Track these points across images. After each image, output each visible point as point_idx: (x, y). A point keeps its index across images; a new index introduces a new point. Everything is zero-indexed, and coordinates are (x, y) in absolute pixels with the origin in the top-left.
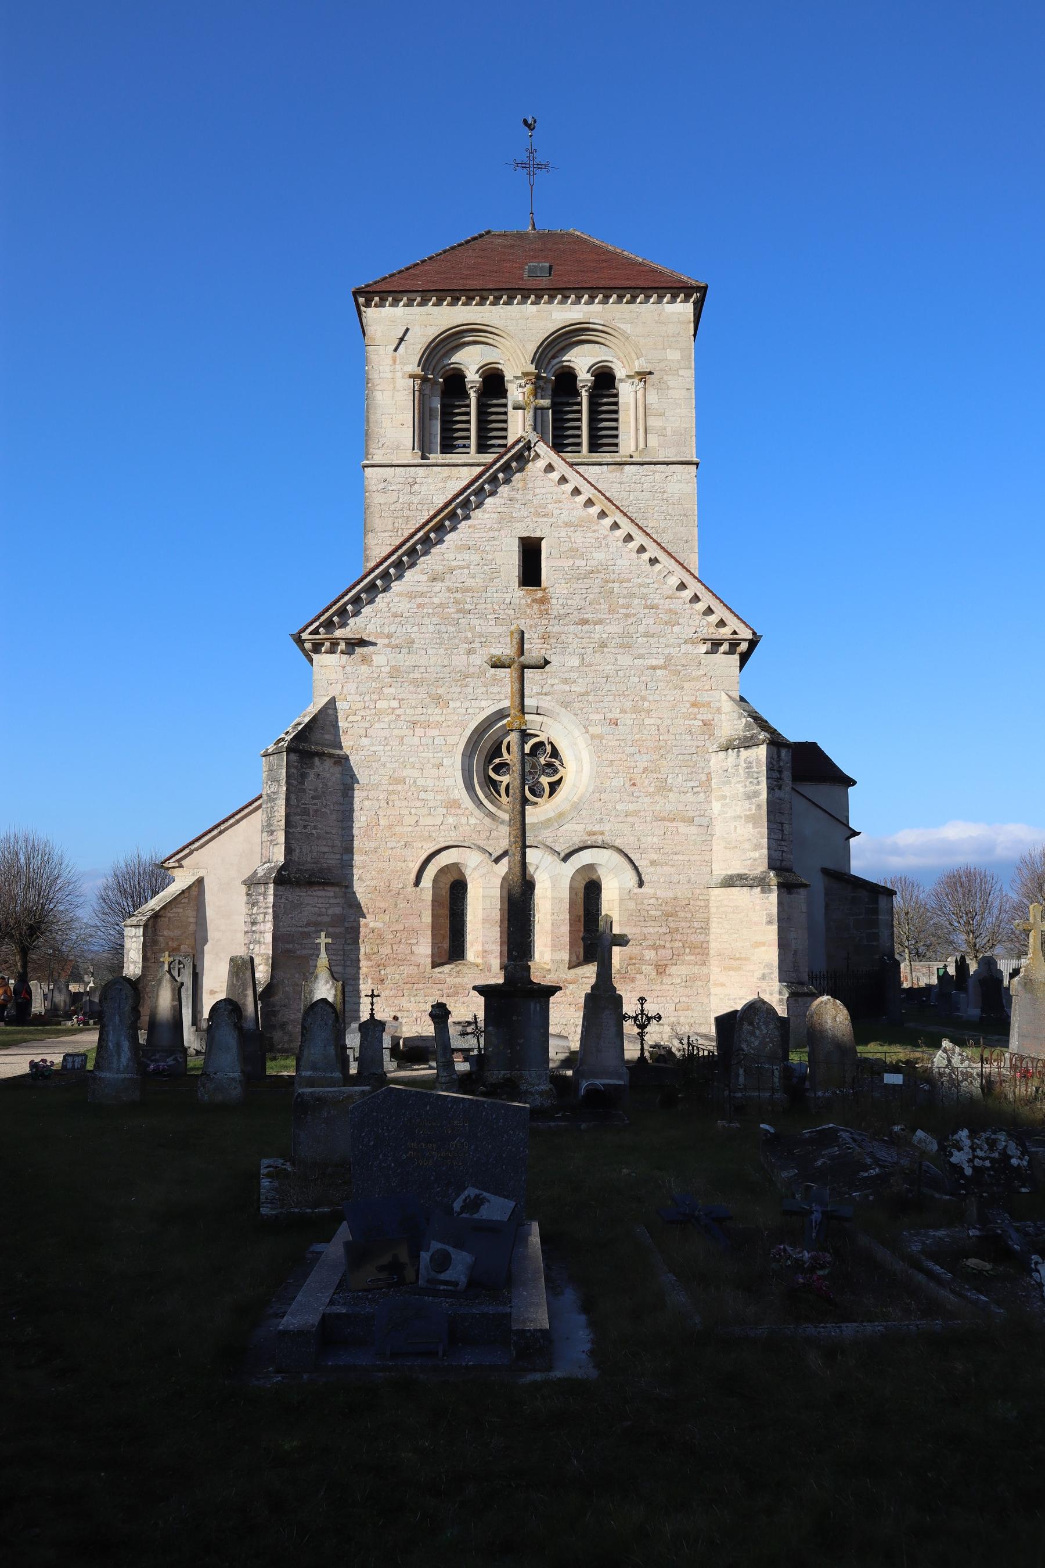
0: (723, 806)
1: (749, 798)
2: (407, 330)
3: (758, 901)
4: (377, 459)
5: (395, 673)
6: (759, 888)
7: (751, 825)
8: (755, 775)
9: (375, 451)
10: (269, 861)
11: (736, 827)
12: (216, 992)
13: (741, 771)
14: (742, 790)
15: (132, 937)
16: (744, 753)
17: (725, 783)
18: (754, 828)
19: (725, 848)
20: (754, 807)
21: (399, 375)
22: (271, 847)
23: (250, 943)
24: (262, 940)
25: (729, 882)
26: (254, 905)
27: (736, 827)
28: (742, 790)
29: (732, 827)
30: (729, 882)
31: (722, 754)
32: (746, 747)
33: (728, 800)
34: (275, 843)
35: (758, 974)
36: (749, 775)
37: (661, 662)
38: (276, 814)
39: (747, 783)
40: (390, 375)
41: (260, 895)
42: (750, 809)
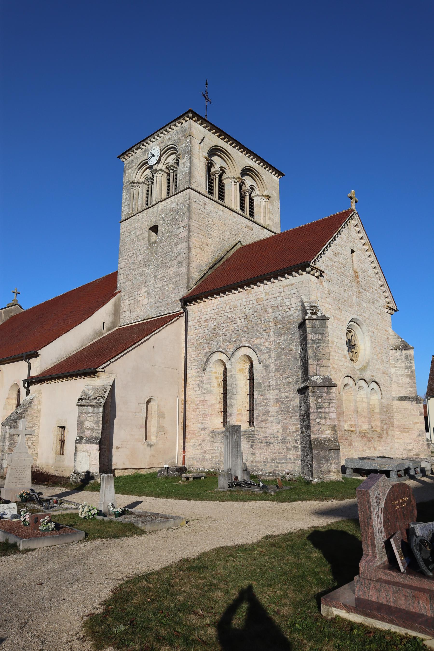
0: (396, 370)
1: (407, 368)
2: (204, 138)
3: (415, 407)
4: (194, 187)
5: (330, 293)
6: (415, 402)
7: (409, 378)
8: (410, 360)
9: (193, 183)
10: (316, 375)
11: (402, 379)
12: (119, 448)
13: (403, 358)
14: (404, 365)
15: (89, 413)
16: (404, 352)
17: (396, 362)
18: (410, 379)
19: (398, 386)
20: (410, 372)
21: (201, 155)
22: (318, 368)
23: (317, 418)
24: (327, 417)
25: (403, 399)
26: (318, 398)
27: (402, 379)
28: (404, 365)
29: (400, 379)
30: (403, 399)
31: (394, 351)
32: (405, 350)
33: (398, 368)
34: (322, 365)
35: (417, 434)
36: (407, 360)
37: (379, 312)
38: (321, 350)
39: (406, 363)
40: (198, 153)
41: (324, 392)
42: (408, 372)
